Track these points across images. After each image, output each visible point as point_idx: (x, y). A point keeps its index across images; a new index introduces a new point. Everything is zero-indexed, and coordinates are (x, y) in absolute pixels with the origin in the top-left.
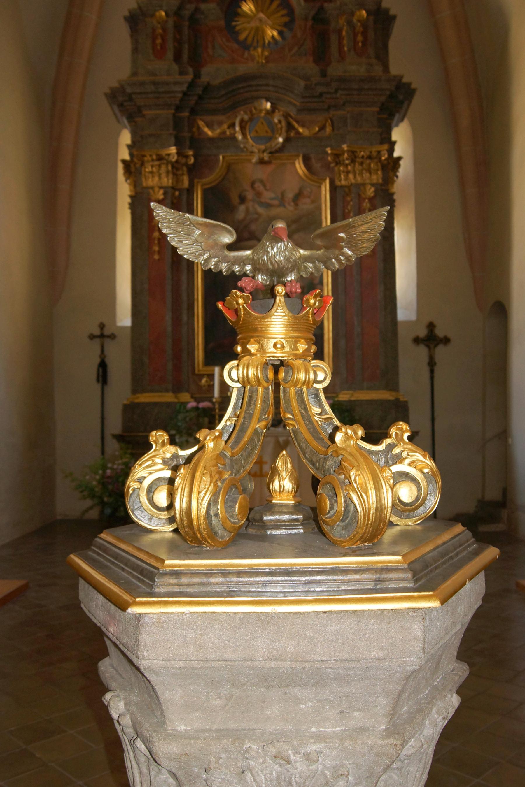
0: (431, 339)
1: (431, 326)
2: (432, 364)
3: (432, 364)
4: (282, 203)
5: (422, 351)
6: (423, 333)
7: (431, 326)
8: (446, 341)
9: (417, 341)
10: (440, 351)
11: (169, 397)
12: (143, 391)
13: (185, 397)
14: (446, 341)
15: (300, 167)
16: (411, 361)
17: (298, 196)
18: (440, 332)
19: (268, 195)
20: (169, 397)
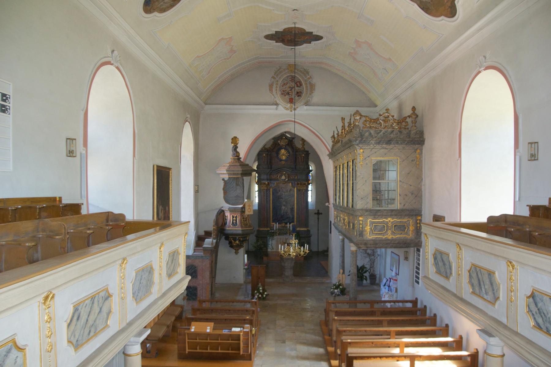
0: (318, 213)
1: (318, 210)
2: (318, 219)
3: (318, 219)
4: (287, 191)
5: (316, 216)
6: (317, 212)
7: (318, 210)
8: (321, 214)
9: (315, 214)
10: (320, 216)
11: (266, 229)
12: (261, 227)
13: (269, 229)
14: (321, 214)
15: (290, 184)
16: (312, 220)
17: (291, 190)
18: (320, 212)
19: (284, 190)
20: (266, 229)
